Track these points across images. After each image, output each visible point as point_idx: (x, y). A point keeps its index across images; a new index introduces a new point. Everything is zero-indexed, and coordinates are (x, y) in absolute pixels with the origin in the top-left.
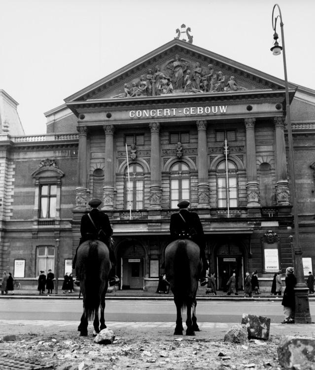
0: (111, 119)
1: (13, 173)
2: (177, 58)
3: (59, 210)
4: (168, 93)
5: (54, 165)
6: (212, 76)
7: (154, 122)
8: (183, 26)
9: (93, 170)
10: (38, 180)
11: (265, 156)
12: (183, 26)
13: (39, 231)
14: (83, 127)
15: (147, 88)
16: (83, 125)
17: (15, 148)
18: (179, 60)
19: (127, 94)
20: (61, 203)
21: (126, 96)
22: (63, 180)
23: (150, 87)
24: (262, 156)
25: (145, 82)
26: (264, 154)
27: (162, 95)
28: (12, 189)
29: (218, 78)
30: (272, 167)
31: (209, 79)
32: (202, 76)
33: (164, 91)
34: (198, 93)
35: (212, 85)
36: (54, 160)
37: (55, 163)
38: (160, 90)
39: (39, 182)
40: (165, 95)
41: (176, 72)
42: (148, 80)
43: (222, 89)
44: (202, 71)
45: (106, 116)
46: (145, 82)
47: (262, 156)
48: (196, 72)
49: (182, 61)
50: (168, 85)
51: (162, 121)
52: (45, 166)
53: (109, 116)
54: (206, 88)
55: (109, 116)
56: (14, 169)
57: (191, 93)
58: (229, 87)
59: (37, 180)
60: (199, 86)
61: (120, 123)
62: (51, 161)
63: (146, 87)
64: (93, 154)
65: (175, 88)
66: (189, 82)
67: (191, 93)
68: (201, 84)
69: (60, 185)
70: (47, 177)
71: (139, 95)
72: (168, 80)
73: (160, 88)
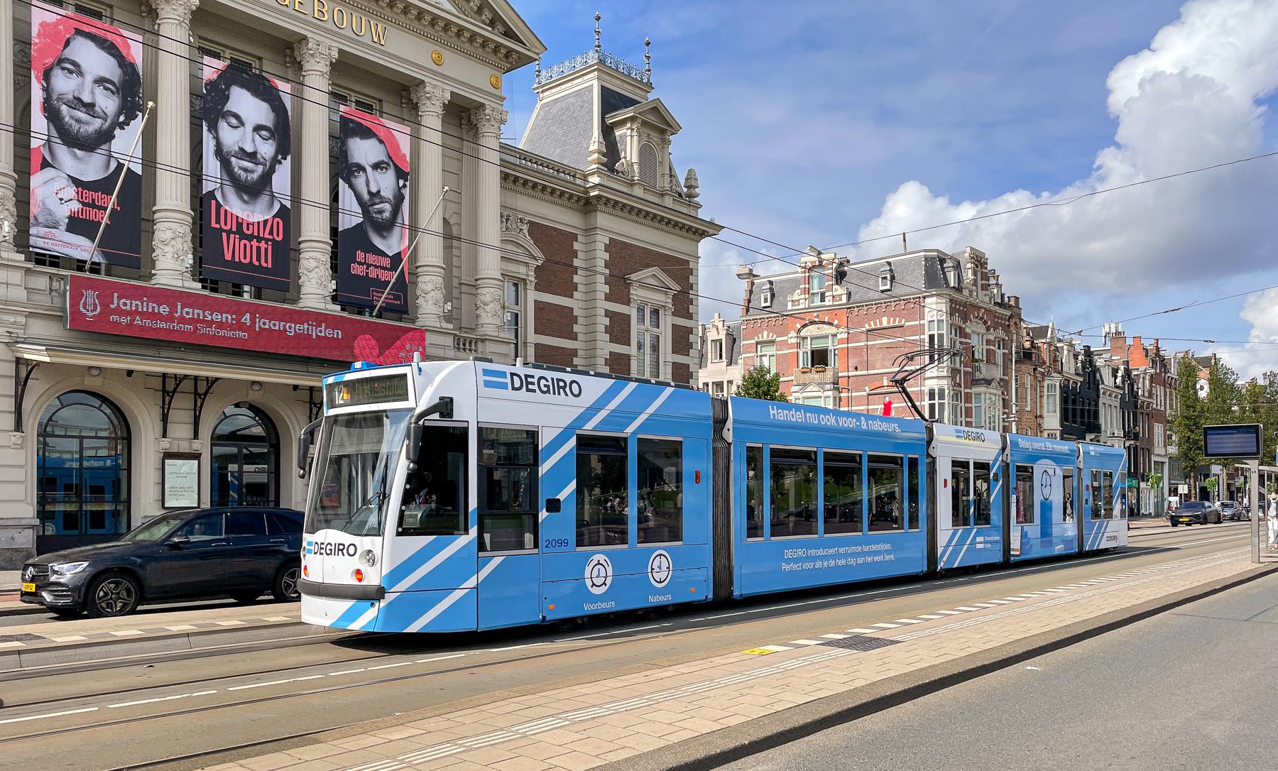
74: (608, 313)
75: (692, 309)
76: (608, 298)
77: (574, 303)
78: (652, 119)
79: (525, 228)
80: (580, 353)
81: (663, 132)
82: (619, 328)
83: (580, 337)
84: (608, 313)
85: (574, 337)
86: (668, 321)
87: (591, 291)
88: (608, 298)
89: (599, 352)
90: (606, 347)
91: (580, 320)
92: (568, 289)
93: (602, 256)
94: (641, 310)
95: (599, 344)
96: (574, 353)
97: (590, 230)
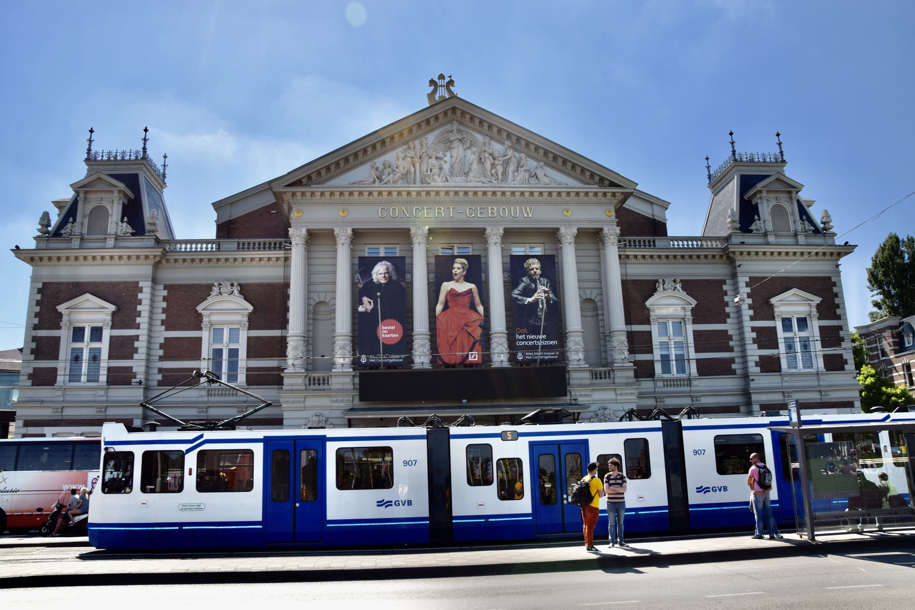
2: (455, 127)
6: (510, 158)
8: (441, 77)
12: (441, 77)
18: (459, 131)
21: (374, 182)
23: (412, 170)
27: (433, 184)
30: (599, 304)
31: (506, 163)
34: (492, 185)
35: (511, 174)
54: (500, 176)
56: (165, 299)
57: (480, 184)
67: (480, 184)
68: (493, 171)
74: (754, 329)
75: (838, 312)
76: (752, 318)
77: (729, 326)
78: (778, 187)
79: (679, 286)
80: (737, 360)
81: (790, 192)
82: (767, 338)
83: (736, 349)
84: (754, 329)
85: (731, 350)
86: (815, 325)
87: (739, 316)
88: (752, 318)
89: (750, 358)
90: (754, 353)
91: (734, 338)
92: (722, 317)
93: (744, 290)
94: (787, 324)
95: (749, 353)
96: (732, 360)
97: (734, 276)
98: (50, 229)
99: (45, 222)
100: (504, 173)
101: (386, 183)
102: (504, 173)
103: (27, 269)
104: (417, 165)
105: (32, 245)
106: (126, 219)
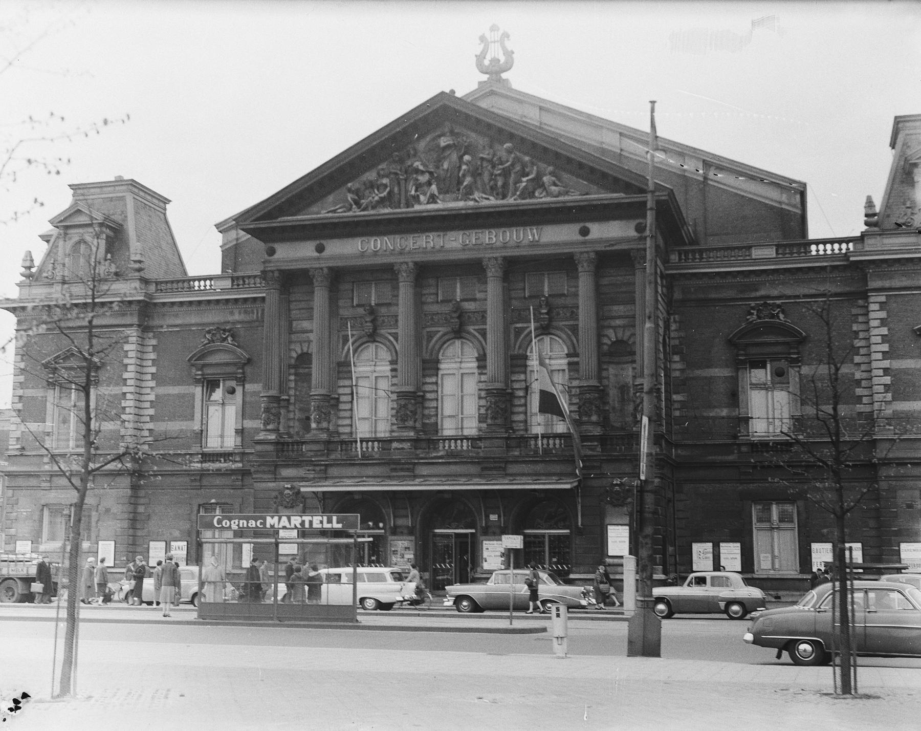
0: (324, 254)
1: (153, 356)
2: (446, 130)
3: (240, 432)
4: (428, 203)
5: (230, 339)
7: (402, 260)
9: (294, 355)
10: (201, 370)
11: (619, 326)
13: (203, 474)
14: (273, 272)
15: (389, 193)
16: (273, 269)
17: (155, 304)
18: (452, 133)
19: (351, 205)
20: (244, 417)
22: (248, 369)
24: (614, 328)
25: (385, 181)
26: (618, 322)
27: (417, 207)
28: (152, 388)
29: (523, 169)
31: (506, 173)
32: (494, 167)
33: (422, 198)
36: (229, 331)
37: (233, 336)
38: (413, 197)
39: (202, 375)
40: (423, 207)
41: (444, 158)
42: (392, 176)
43: (532, 195)
44: (494, 155)
45: (314, 248)
46: (385, 181)
47: (614, 328)
48: (482, 159)
49: (458, 133)
50: (429, 184)
51: (419, 258)
52: (213, 341)
53: (320, 249)
55: (320, 249)
57: (471, 203)
58: (545, 189)
59: (198, 370)
60: (488, 187)
61: (340, 264)
62: (224, 330)
63: (388, 189)
64: (294, 324)
65: (443, 191)
66: (468, 180)
67: (471, 203)
69: (242, 381)
70: (217, 365)
71: (373, 208)
72: (431, 173)
73: (413, 193)
98: (34, 270)
99: (28, 264)
100: (505, 185)
101: (363, 210)
102: (505, 185)
103: (12, 319)
104: (402, 183)
105: (14, 293)
106: (109, 256)
